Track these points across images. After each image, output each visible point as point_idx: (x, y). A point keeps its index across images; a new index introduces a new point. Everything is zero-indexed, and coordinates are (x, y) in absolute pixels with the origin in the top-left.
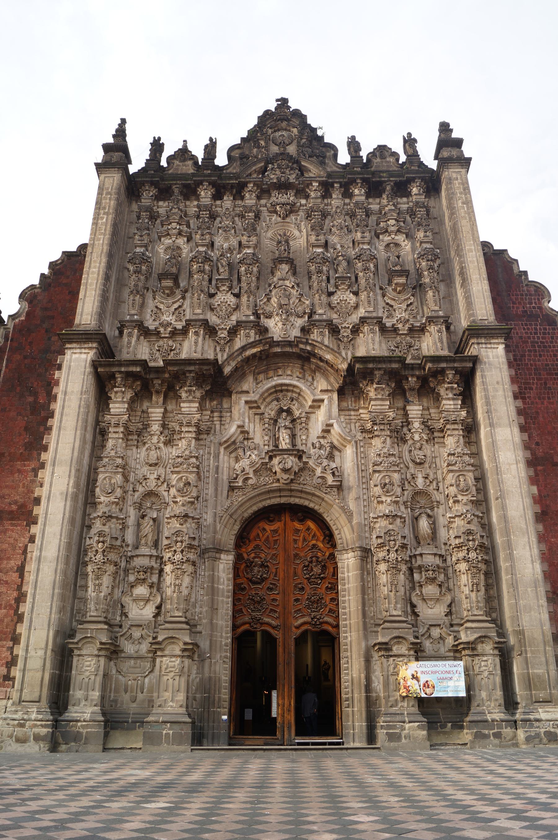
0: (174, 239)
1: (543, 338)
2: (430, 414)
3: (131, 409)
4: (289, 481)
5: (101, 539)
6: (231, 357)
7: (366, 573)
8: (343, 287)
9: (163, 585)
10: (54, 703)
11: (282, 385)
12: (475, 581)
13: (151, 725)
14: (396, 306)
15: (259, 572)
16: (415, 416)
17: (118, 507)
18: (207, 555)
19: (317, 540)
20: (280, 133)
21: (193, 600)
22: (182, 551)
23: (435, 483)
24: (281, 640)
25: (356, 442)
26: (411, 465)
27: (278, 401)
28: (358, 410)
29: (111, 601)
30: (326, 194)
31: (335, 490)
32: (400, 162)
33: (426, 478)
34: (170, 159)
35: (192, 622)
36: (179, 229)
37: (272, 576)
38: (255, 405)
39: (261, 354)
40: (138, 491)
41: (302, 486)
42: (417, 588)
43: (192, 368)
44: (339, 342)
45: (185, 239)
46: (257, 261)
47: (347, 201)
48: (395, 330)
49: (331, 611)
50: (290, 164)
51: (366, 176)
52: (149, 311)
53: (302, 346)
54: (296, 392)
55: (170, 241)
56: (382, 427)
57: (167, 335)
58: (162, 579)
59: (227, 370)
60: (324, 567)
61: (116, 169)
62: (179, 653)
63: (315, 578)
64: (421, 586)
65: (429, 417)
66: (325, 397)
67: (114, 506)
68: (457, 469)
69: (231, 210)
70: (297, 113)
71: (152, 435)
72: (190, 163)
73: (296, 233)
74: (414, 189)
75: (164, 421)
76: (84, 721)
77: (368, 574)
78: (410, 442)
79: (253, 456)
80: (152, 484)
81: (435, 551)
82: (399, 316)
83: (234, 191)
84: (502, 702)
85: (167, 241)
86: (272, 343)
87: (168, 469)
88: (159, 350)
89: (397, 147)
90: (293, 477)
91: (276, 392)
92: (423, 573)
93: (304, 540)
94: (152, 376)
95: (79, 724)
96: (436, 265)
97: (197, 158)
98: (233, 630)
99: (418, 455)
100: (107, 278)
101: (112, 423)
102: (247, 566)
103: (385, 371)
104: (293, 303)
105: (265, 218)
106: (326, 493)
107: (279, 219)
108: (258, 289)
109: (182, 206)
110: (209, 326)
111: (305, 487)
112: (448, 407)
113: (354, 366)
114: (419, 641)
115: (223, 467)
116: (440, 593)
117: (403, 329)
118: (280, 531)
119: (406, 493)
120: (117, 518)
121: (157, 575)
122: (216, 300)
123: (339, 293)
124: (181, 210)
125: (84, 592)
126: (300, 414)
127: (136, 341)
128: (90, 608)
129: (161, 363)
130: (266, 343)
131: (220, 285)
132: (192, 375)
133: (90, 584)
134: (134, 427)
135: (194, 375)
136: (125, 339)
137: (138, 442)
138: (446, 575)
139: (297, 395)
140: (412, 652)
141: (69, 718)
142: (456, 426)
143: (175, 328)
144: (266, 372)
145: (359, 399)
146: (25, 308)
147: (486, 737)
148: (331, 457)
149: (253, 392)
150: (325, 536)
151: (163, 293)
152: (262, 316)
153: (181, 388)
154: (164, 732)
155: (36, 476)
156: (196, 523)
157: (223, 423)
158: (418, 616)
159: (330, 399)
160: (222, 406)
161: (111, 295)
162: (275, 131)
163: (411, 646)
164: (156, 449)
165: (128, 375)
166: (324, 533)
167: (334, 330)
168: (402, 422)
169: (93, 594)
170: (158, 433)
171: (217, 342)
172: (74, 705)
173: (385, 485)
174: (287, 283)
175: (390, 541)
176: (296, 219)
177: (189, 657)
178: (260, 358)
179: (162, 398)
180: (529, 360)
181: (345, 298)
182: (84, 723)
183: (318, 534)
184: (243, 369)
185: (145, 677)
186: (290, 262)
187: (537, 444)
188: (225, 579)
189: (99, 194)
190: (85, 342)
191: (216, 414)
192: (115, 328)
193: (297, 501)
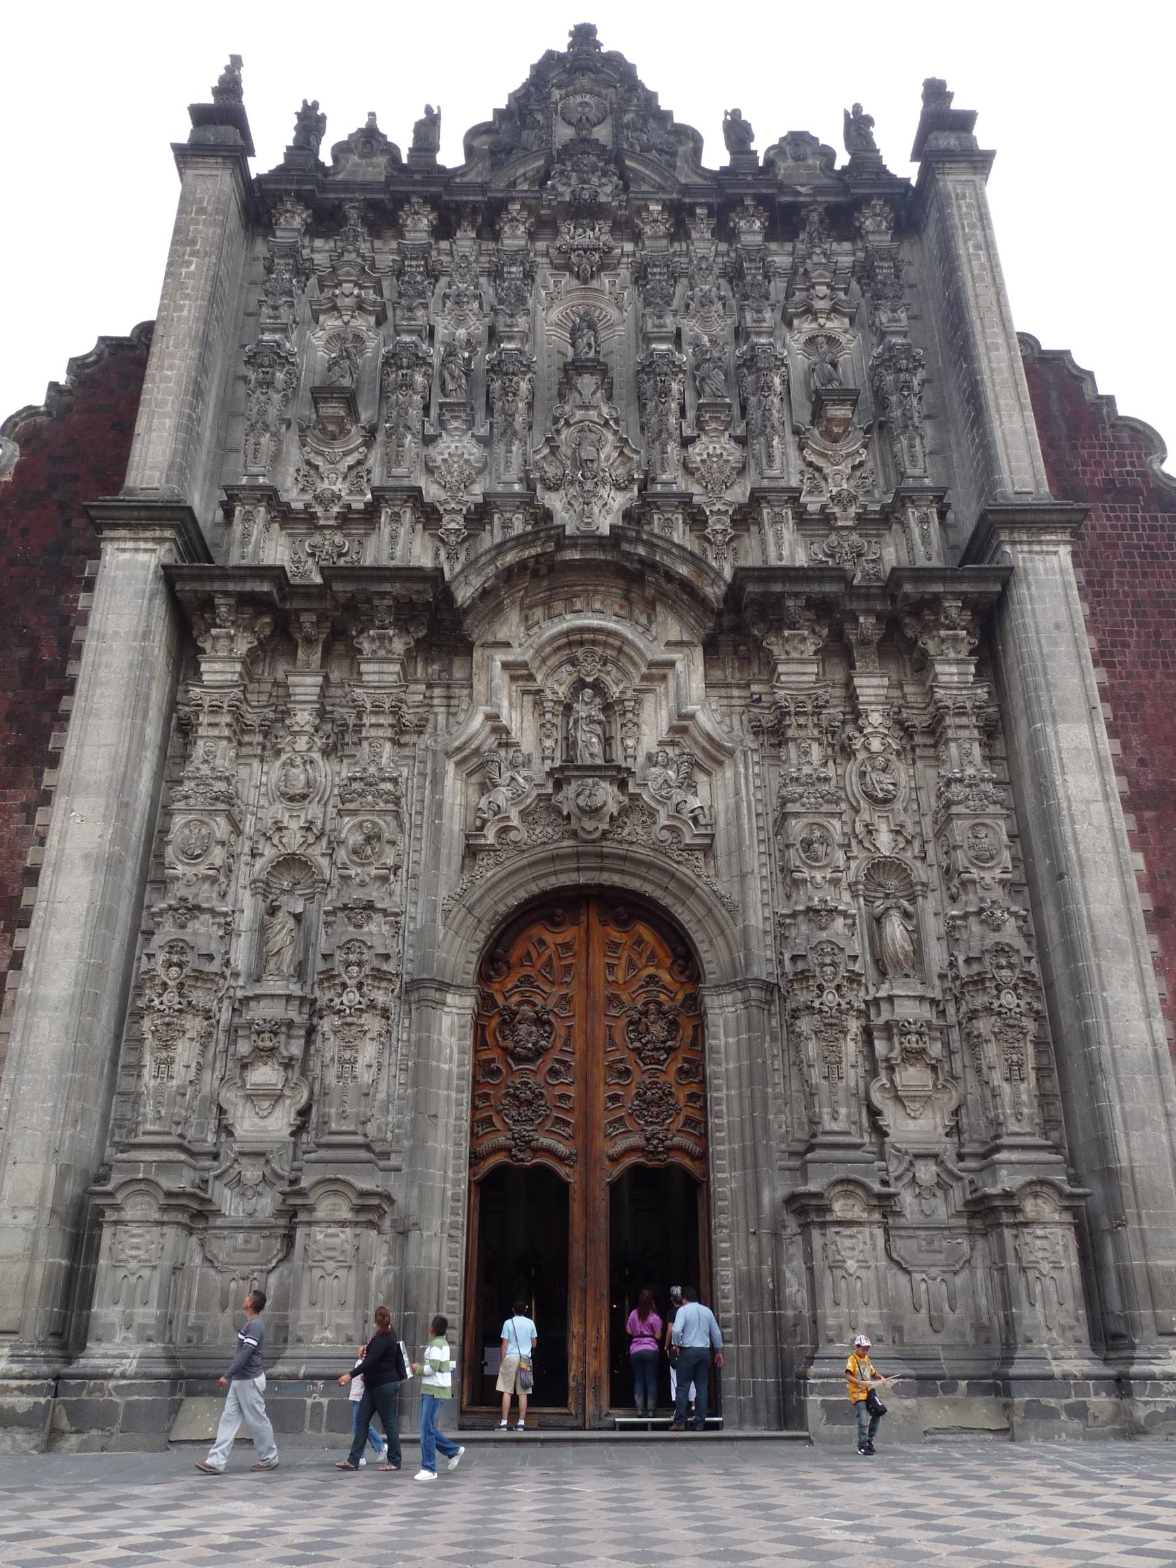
0: (346, 318)
1: (1149, 538)
2: (904, 696)
3: (249, 674)
4: (597, 835)
5: (175, 958)
6: (470, 565)
8: (714, 425)
9: (315, 1063)
10: (53, 1334)
11: (582, 630)
13: (279, 1385)
14: (828, 469)
15: (530, 1034)
16: (873, 699)
17: (216, 887)
18: (414, 997)
19: (657, 967)
20: (579, 99)
21: (381, 1096)
23: (917, 844)
24: (576, 1187)
25: (745, 753)
27: (574, 665)
28: (748, 686)
29: (194, 1097)
30: (679, 232)
31: (700, 855)
32: (838, 166)
33: (898, 832)
34: (340, 150)
35: (378, 1147)
36: (358, 296)
37: (559, 1044)
38: (525, 672)
39: (537, 562)
40: (262, 855)
41: (626, 846)
42: (883, 1074)
43: (387, 587)
44: (706, 545)
45: (372, 319)
46: (528, 366)
47: (723, 247)
48: (826, 519)
49: (689, 1121)
50: (601, 164)
51: (764, 191)
52: (292, 470)
53: (625, 547)
54: (612, 647)
55: (339, 323)
56: (802, 721)
57: (331, 522)
58: (312, 1049)
60: (673, 1025)
61: (220, 160)
63: (656, 1049)
64: (891, 1069)
65: (901, 702)
66: (675, 656)
67: (206, 886)
68: (967, 811)
69: (472, 259)
70: (615, 61)
72: (382, 160)
73: (613, 313)
74: (868, 223)
75: (322, 704)
76: (123, 1376)
77: (774, 1039)
78: (861, 756)
79: (521, 780)
80: (293, 840)
81: (920, 990)
82: (835, 490)
83: (480, 219)
84: (1083, 1331)
85: (331, 323)
86: (561, 540)
87: (330, 809)
88: (313, 555)
89: (832, 136)
90: (606, 827)
91: (570, 644)
92: (896, 1039)
93: (631, 965)
94: (297, 604)
95: (111, 1384)
96: (916, 382)
97: (396, 149)
98: (471, 1165)
99: (880, 782)
100: (198, 393)
101: (206, 705)
102: (504, 1022)
103: (808, 599)
104: (607, 459)
105: (545, 279)
106: (678, 863)
107: (575, 283)
108: (530, 428)
109: (364, 247)
110: (423, 504)
111: (634, 848)
113: (742, 588)
114: (892, 1190)
116: (935, 1085)
117: (845, 517)
118: (576, 947)
119: (853, 864)
120: (213, 912)
121: (302, 1041)
122: (438, 450)
123: (704, 438)
124: (363, 257)
125: (133, 1080)
127: (260, 533)
128: (145, 1115)
129: (318, 580)
130: (549, 538)
131: (447, 416)
132: (385, 602)
133: (148, 1060)
134: (255, 717)
135: (390, 603)
136: (238, 527)
137: (264, 748)
138: (946, 1045)
139: (614, 653)
140: (877, 1216)
141: (88, 1371)
142: (964, 721)
143: (349, 507)
144: (547, 603)
145: (749, 661)
146: (13, 456)
147: (1050, 1414)
148: (689, 785)
149: (520, 645)
150: (676, 956)
151: (323, 431)
152: (539, 486)
153: (361, 632)
154: (309, 1401)
155: (30, 820)
156: (391, 924)
157: (452, 710)
158: (886, 1134)
159: (689, 662)
160: (451, 675)
161: (208, 434)
162: (567, 95)
163: (875, 1202)
164: (305, 763)
165: (245, 600)
166: (674, 950)
167: (697, 519)
168: (844, 714)
169: (152, 1083)
171: (442, 540)
172: (99, 1340)
174: (593, 413)
176: (613, 284)
177: (371, 1224)
178: (535, 574)
179: (319, 655)
180: (1121, 584)
182: (123, 1382)
183: (660, 953)
184: (498, 596)
185: (269, 1272)
186: (600, 369)
187: (1142, 762)
188: (455, 1050)
189: (181, 211)
190: (146, 527)
191: (437, 692)
192: (216, 505)
193: (616, 879)
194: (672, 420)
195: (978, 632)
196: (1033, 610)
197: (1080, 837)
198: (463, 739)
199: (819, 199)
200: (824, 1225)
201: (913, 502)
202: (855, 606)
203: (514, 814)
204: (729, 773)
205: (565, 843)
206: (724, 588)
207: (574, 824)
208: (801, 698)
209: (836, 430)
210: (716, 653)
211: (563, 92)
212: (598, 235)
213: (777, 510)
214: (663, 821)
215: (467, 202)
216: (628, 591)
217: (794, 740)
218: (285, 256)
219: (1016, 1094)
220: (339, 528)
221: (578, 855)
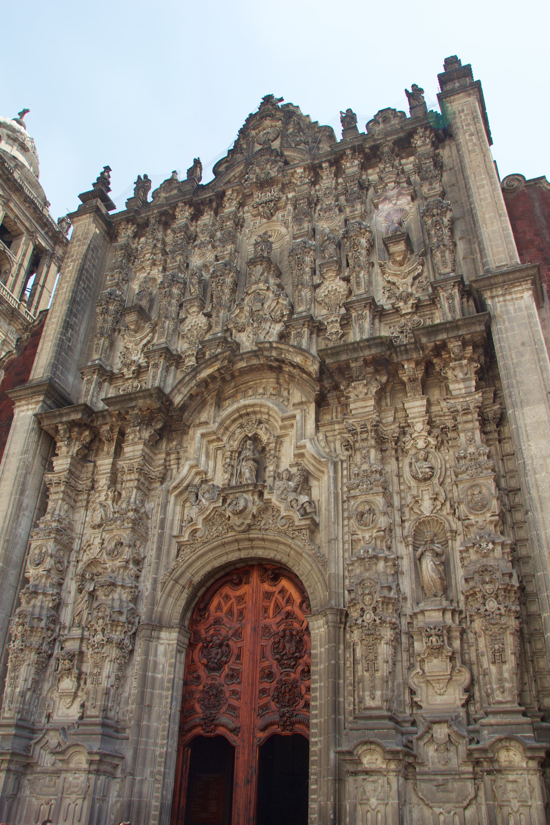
0: (148, 271)
7: (342, 646)
8: (330, 274)
11: (245, 407)
12: (497, 647)
16: (417, 414)
22: (103, 630)
26: (413, 483)
34: (156, 194)
36: (153, 258)
38: (214, 437)
39: (221, 374)
40: (82, 560)
41: (263, 532)
43: (133, 404)
56: (364, 436)
57: (131, 376)
59: (178, 399)
62: (85, 766)
85: (142, 275)
90: (248, 521)
91: (241, 416)
93: (277, 606)
103: (365, 361)
104: (269, 307)
107: (265, 221)
110: (172, 355)
115: (173, 521)
118: (247, 598)
122: (186, 325)
123: (326, 283)
124: (158, 240)
126: (269, 439)
134: (84, 486)
137: (88, 502)
139: (266, 417)
142: (469, 417)
144: (233, 396)
152: (234, 331)
165: (72, 424)
170: (106, 488)
173: (362, 514)
175: (363, 595)
179: (114, 447)
181: (334, 288)
191: (173, 456)
194: (307, 277)
195: (482, 359)
196: (507, 337)
197: (539, 483)
198: (177, 481)
199: (388, 139)
200: (355, 773)
201: (442, 288)
202: (399, 359)
203: (200, 519)
204: (326, 478)
205: (230, 534)
206: (318, 365)
207: (231, 522)
208: (362, 423)
209: (398, 259)
210: (328, 405)
211: (257, 131)
212: (273, 192)
213: (360, 312)
214: (283, 514)
215: (206, 198)
216: (278, 379)
217: (359, 449)
218: (122, 249)
219: (500, 673)
220: (135, 378)
221: (237, 541)
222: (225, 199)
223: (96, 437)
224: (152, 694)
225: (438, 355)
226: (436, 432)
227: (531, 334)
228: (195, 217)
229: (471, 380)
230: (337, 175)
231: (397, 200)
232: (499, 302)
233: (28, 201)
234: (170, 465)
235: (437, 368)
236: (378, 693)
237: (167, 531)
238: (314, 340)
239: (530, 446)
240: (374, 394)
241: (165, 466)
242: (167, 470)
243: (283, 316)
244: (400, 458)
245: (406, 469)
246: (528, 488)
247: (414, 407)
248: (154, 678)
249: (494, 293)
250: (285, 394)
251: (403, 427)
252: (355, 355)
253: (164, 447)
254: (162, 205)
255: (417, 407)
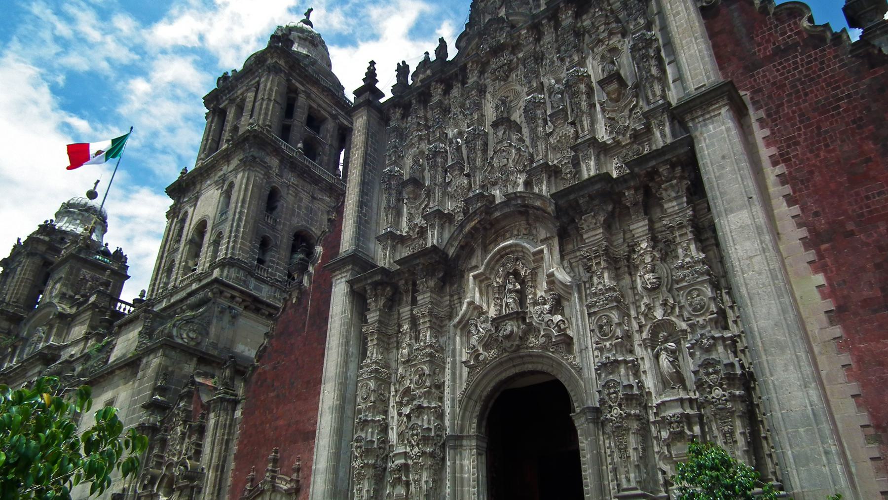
4: (514, 348)
16: (642, 234)
39: (482, 225)
43: (418, 261)
59: (451, 252)
71: (405, 334)
90: (517, 343)
91: (502, 257)
103: (590, 196)
107: (502, 83)
112: (671, 210)
126: (525, 273)
165: (375, 285)
191: (456, 297)
197: (747, 281)
209: (613, 96)
210: (569, 236)
214: (542, 333)
215: (452, 74)
216: (527, 220)
218: (394, 132)
222: (468, 71)
223: (396, 291)
224: (462, 491)
225: (652, 179)
226: (661, 245)
227: (730, 146)
228: (446, 92)
229: (683, 197)
230: (556, 29)
231: (609, 40)
232: (699, 122)
233: (325, 90)
234: (454, 304)
235: (654, 191)
236: (632, 476)
237: (457, 358)
238: (553, 182)
239: (736, 249)
240: (602, 222)
241: (451, 306)
242: (453, 309)
243: (525, 166)
244: (633, 273)
245: (639, 281)
246: (738, 287)
247: (638, 228)
248: (462, 478)
249: (695, 115)
250: (534, 232)
251: (632, 246)
252: (582, 193)
253: (448, 290)
254: (419, 87)
255: (641, 227)
